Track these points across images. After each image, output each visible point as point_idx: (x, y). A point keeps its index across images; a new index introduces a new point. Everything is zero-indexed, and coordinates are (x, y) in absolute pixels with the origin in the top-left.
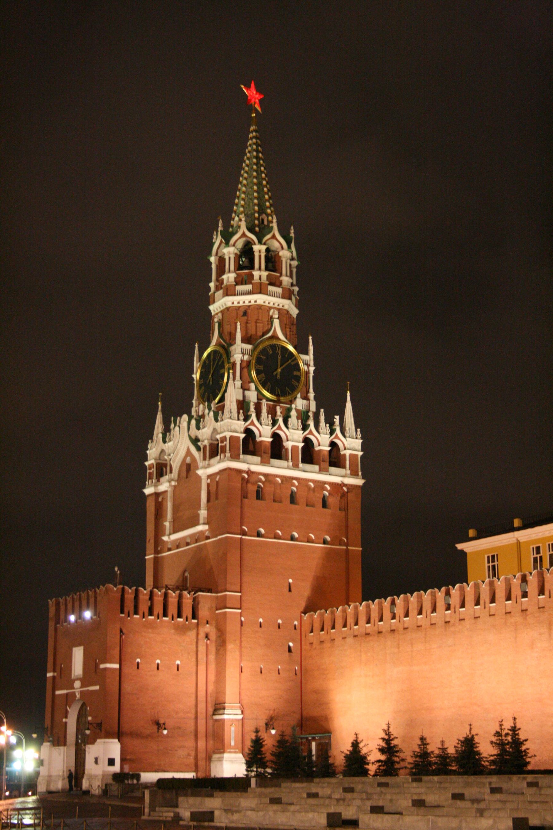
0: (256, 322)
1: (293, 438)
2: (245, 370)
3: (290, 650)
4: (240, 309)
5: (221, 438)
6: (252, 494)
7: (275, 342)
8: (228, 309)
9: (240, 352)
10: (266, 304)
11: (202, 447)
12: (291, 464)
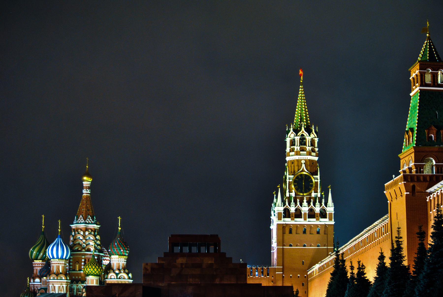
1: (305, 209)
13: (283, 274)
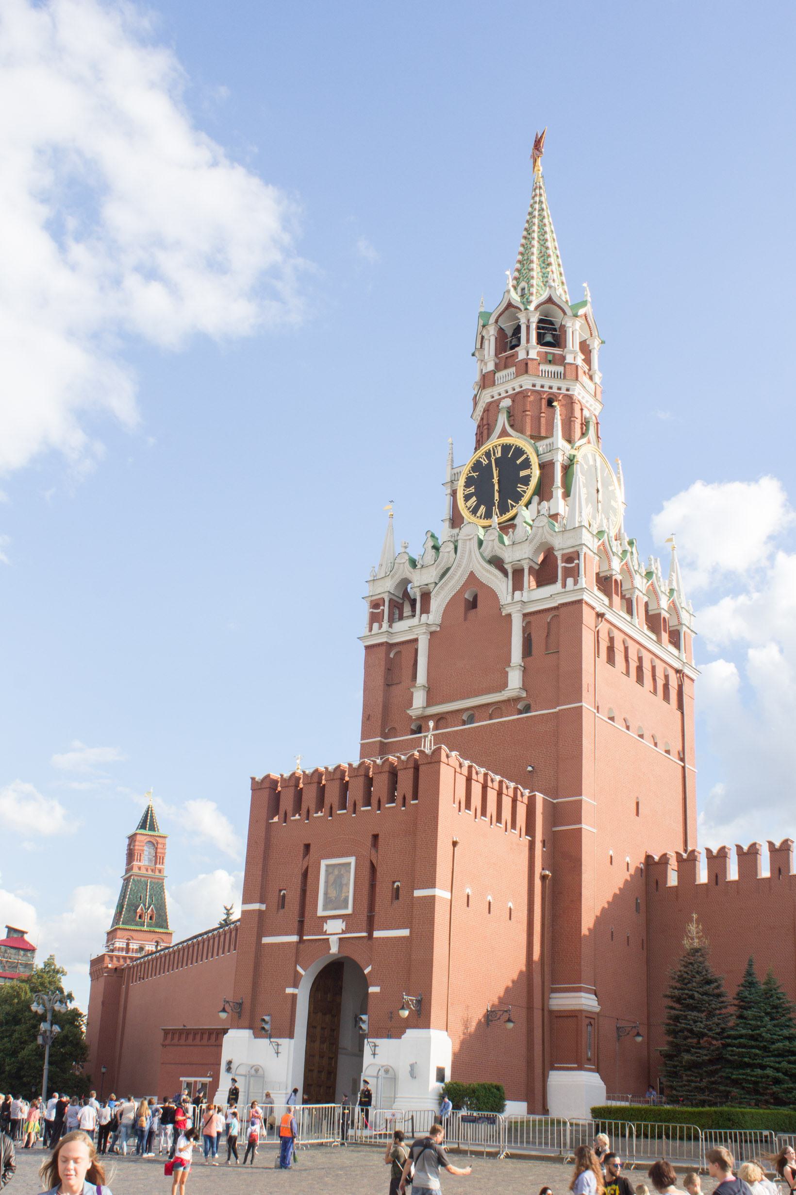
5: (563, 555)
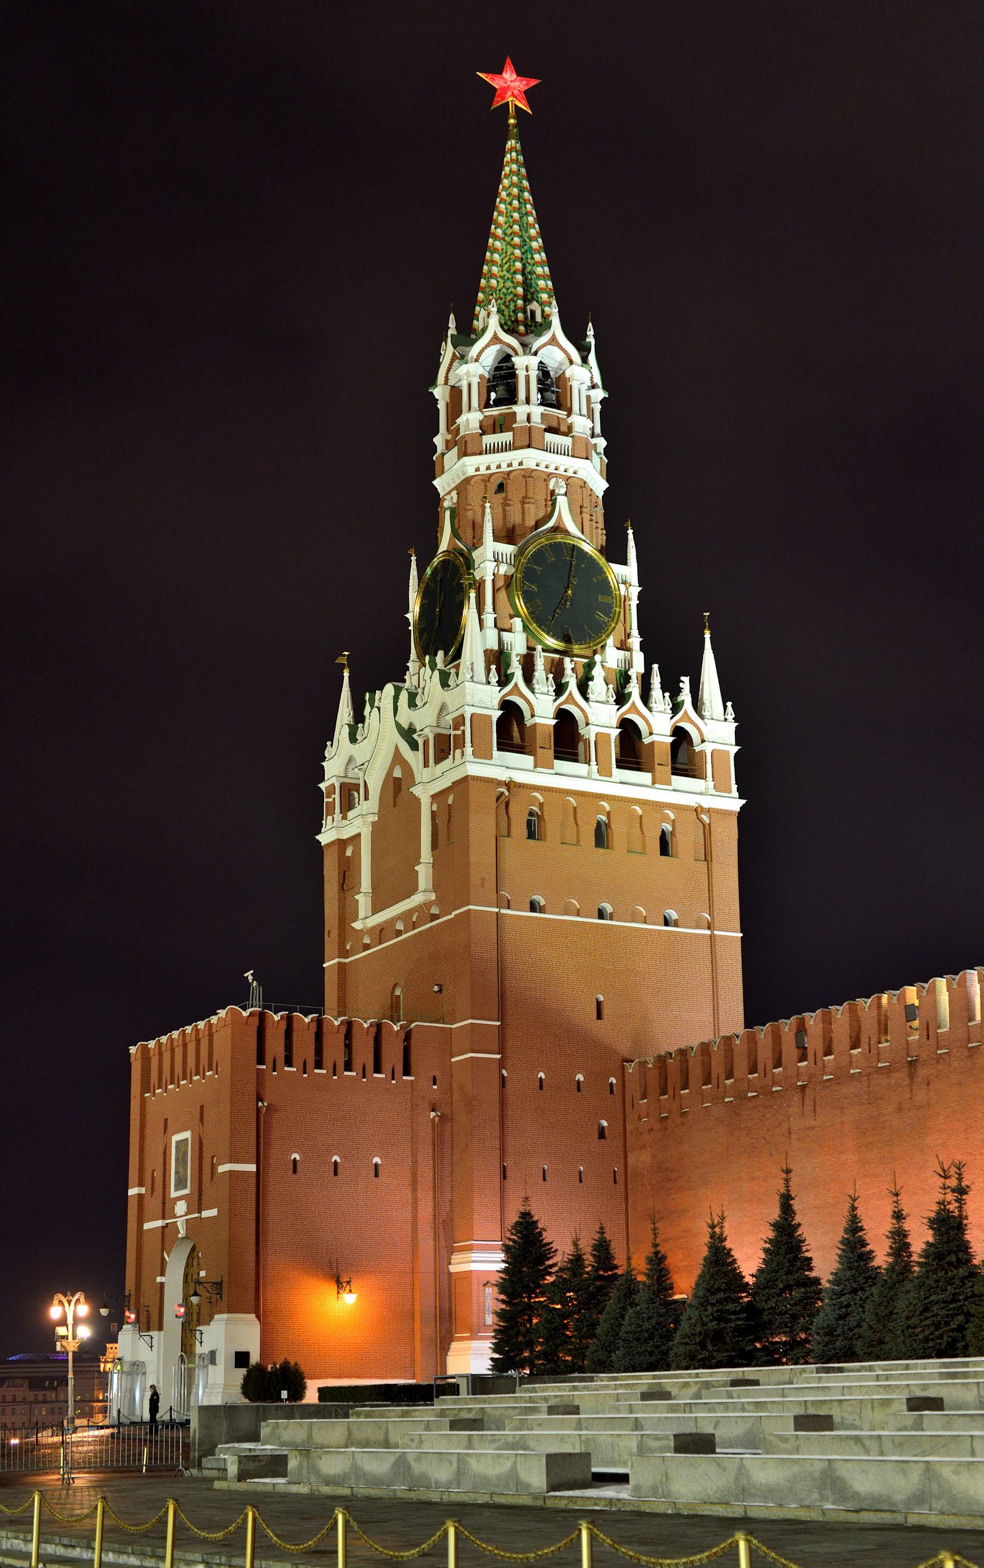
0: (523, 503)
1: (600, 717)
2: (502, 595)
3: (602, 1134)
4: (492, 480)
6: (519, 829)
7: (559, 538)
8: (467, 481)
9: (492, 559)
10: (542, 468)
11: (421, 742)
12: (594, 767)
13: (502, 1064)
